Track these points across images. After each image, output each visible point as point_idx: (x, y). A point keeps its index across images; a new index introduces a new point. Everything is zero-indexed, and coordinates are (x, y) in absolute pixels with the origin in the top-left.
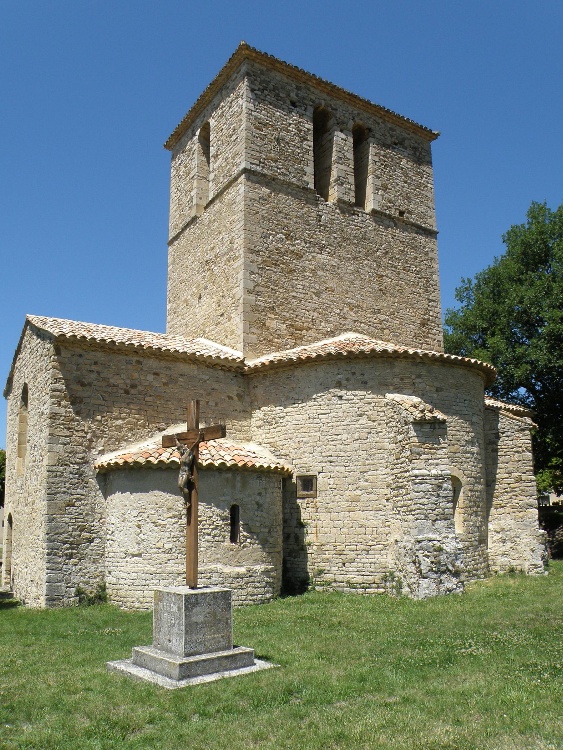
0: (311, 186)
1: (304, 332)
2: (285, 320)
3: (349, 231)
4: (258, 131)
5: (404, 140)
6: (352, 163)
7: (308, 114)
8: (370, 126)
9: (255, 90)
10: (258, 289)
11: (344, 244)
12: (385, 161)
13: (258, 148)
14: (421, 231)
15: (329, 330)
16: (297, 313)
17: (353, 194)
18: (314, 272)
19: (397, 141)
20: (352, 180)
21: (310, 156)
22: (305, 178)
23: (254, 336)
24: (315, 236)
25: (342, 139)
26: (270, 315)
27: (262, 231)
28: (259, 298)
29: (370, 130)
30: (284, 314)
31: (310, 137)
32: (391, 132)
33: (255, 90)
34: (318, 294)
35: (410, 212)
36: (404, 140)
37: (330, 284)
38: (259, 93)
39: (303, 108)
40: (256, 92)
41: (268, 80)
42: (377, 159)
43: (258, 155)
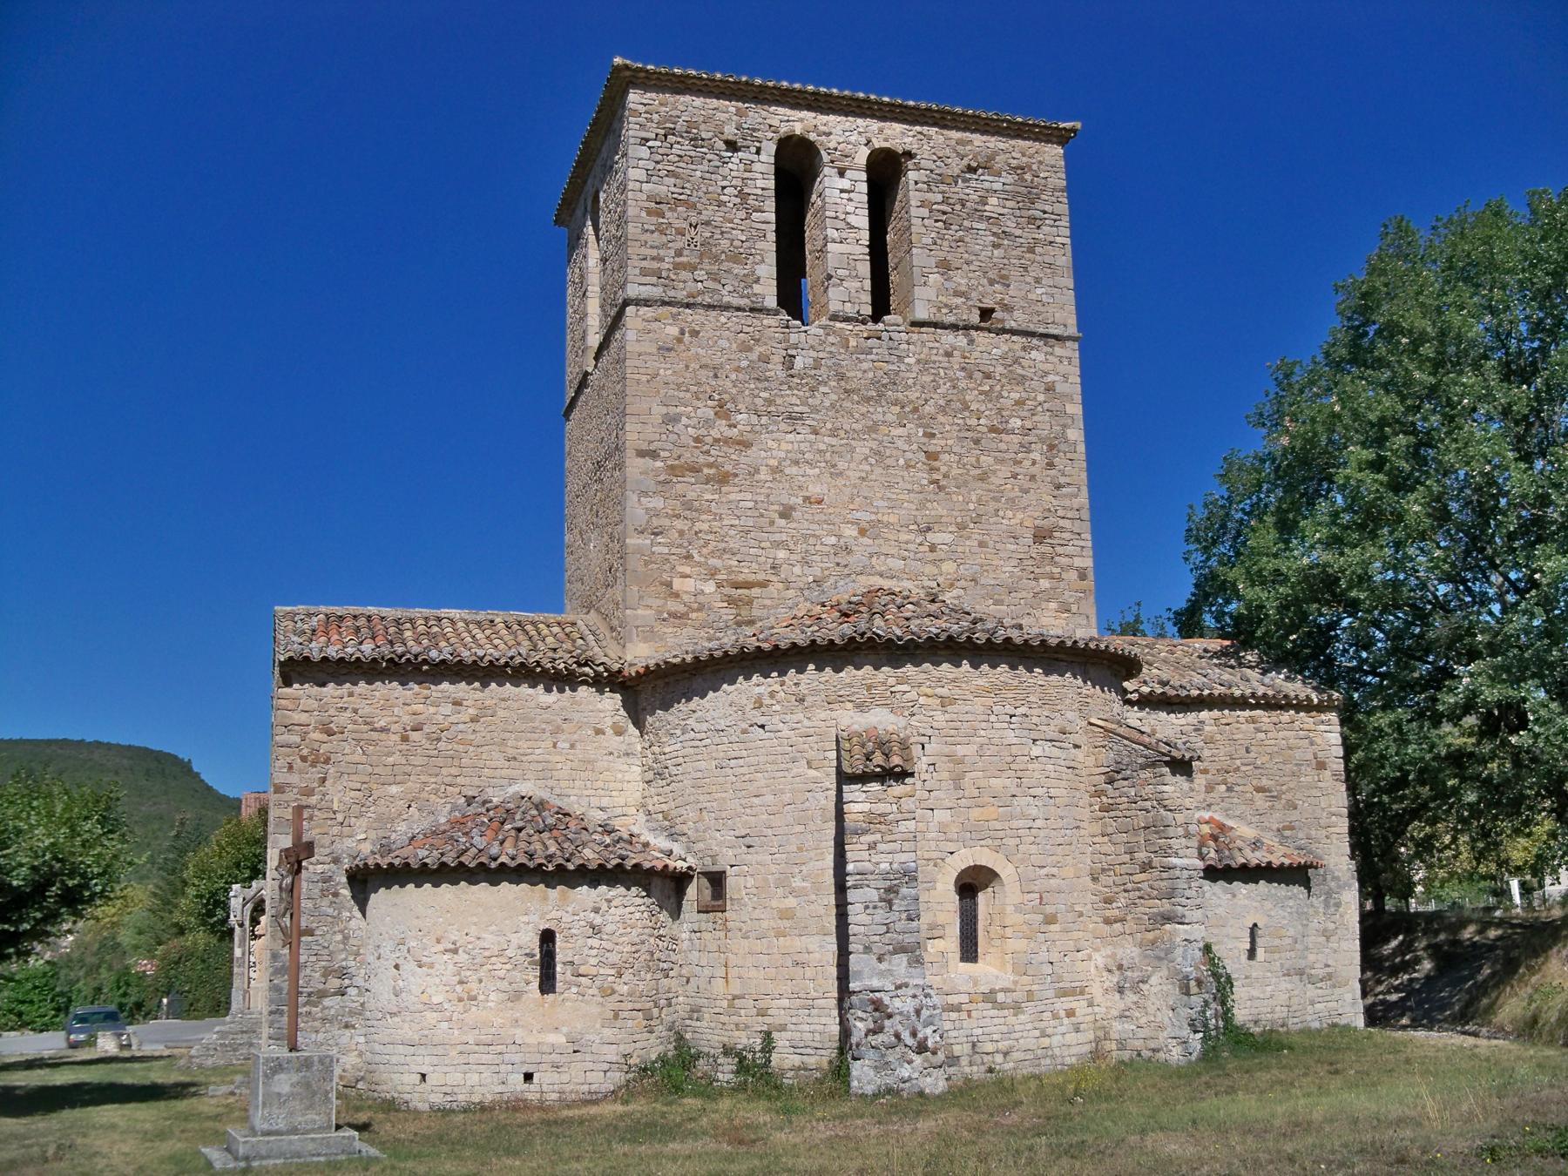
0: (771, 302)
1: (756, 591)
2: (713, 573)
3: (859, 375)
4: (654, 219)
5: (991, 158)
6: (865, 236)
7: (763, 157)
8: (908, 148)
9: (647, 140)
10: (655, 522)
11: (847, 404)
12: (944, 213)
13: (654, 252)
14: (1035, 341)
15: (811, 579)
16: (738, 557)
17: (868, 298)
18: (776, 470)
19: (974, 164)
20: (865, 269)
21: (769, 246)
22: (757, 288)
23: (648, 612)
24: (779, 401)
25: (842, 191)
26: (680, 569)
27: (664, 410)
28: (660, 539)
29: (909, 155)
30: (712, 562)
31: (770, 205)
32: (959, 148)
33: (647, 140)
34: (786, 514)
35: (1008, 308)
36: (991, 158)
37: (815, 490)
38: (658, 143)
39: (753, 150)
40: (650, 144)
41: (674, 113)
42: (925, 212)
43: (655, 265)
